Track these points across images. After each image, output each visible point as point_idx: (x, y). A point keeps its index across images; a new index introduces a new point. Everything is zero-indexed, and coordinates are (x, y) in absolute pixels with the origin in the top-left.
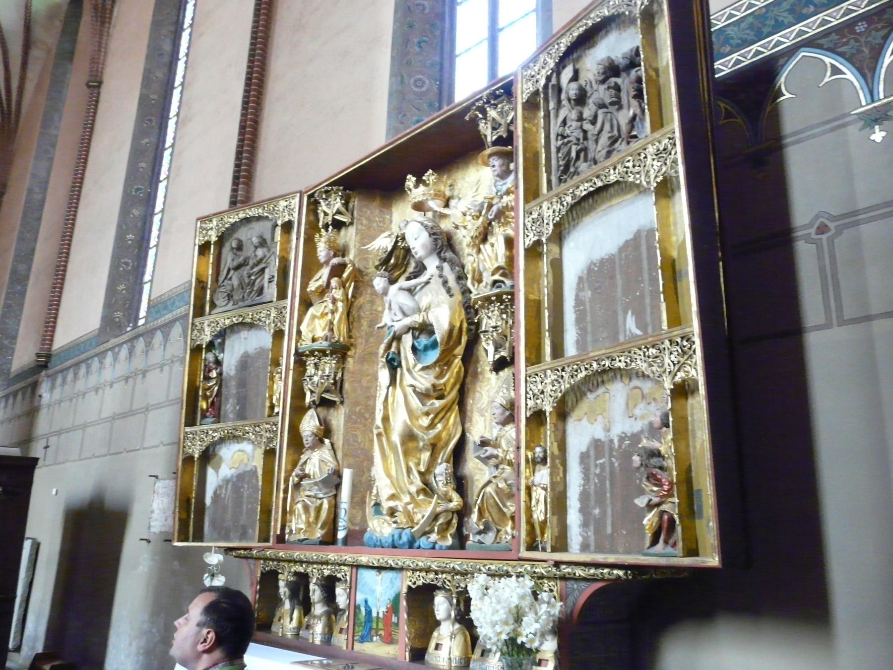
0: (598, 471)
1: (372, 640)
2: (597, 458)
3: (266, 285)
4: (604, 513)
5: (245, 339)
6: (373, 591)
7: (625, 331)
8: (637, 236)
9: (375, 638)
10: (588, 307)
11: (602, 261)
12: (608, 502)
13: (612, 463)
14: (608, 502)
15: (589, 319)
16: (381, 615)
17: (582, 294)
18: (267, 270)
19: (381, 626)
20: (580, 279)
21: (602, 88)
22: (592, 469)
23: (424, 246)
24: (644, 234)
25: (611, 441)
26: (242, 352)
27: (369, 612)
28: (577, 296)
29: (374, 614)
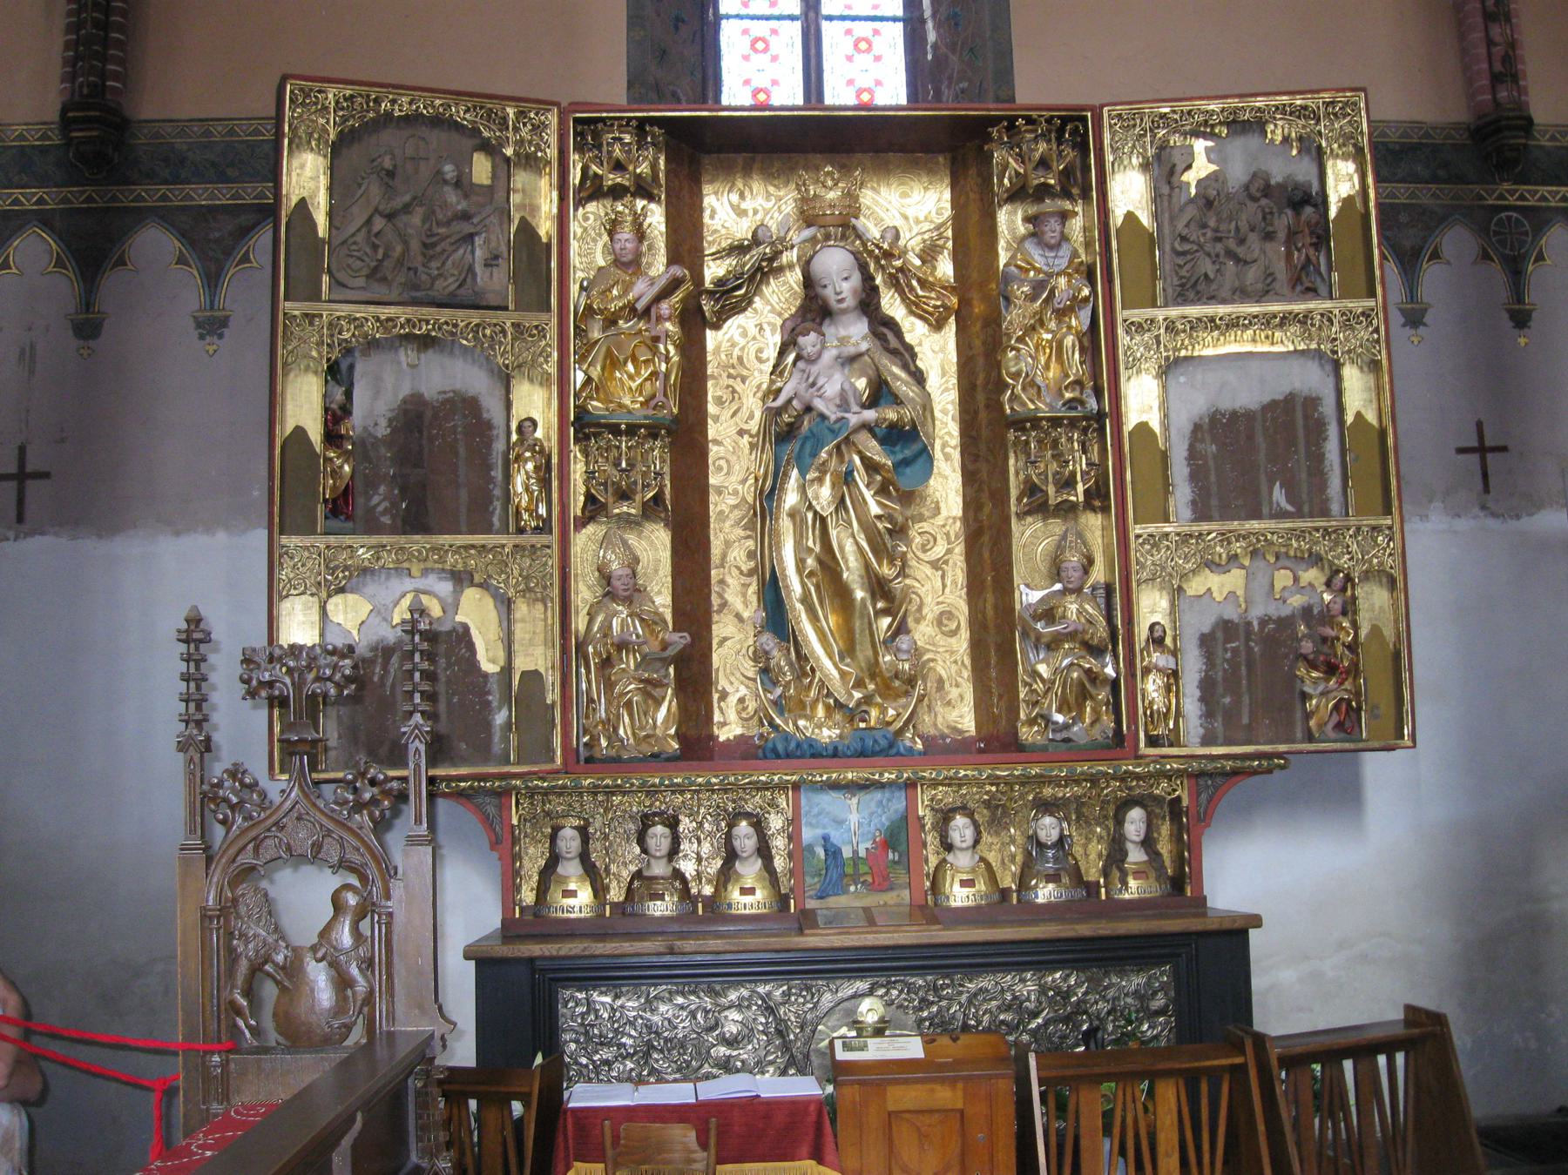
0: (1229, 655)
1: (846, 892)
2: (1227, 641)
3: (478, 269)
4: (1237, 702)
5: (413, 367)
6: (840, 822)
7: (1271, 502)
8: (1290, 399)
9: (852, 888)
10: (1211, 463)
11: (1234, 415)
12: (1244, 689)
13: (1249, 650)
14: (1244, 689)
15: (1213, 478)
16: (862, 854)
17: (1199, 446)
18: (478, 241)
19: (863, 868)
20: (1197, 428)
21: (1252, 206)
22: (1220, 652)
23: (855, 292)
24: (1299, 401)
25: (1249, 624)
26: (405, 390)
27: (833, 853)
28: (1191, 448)
29: (847, 853)
